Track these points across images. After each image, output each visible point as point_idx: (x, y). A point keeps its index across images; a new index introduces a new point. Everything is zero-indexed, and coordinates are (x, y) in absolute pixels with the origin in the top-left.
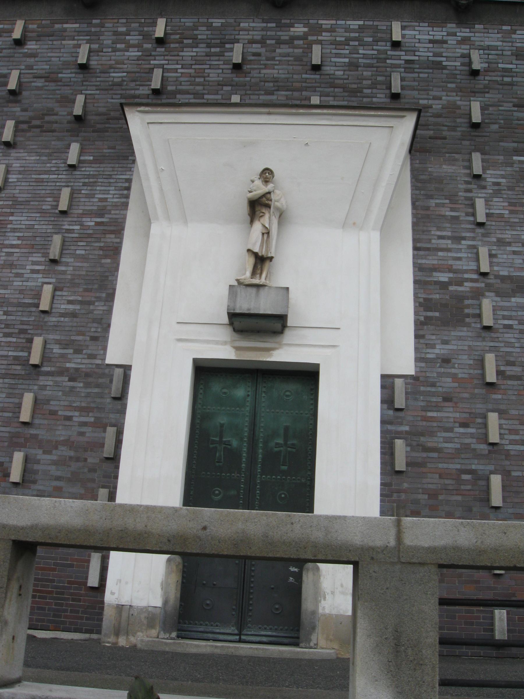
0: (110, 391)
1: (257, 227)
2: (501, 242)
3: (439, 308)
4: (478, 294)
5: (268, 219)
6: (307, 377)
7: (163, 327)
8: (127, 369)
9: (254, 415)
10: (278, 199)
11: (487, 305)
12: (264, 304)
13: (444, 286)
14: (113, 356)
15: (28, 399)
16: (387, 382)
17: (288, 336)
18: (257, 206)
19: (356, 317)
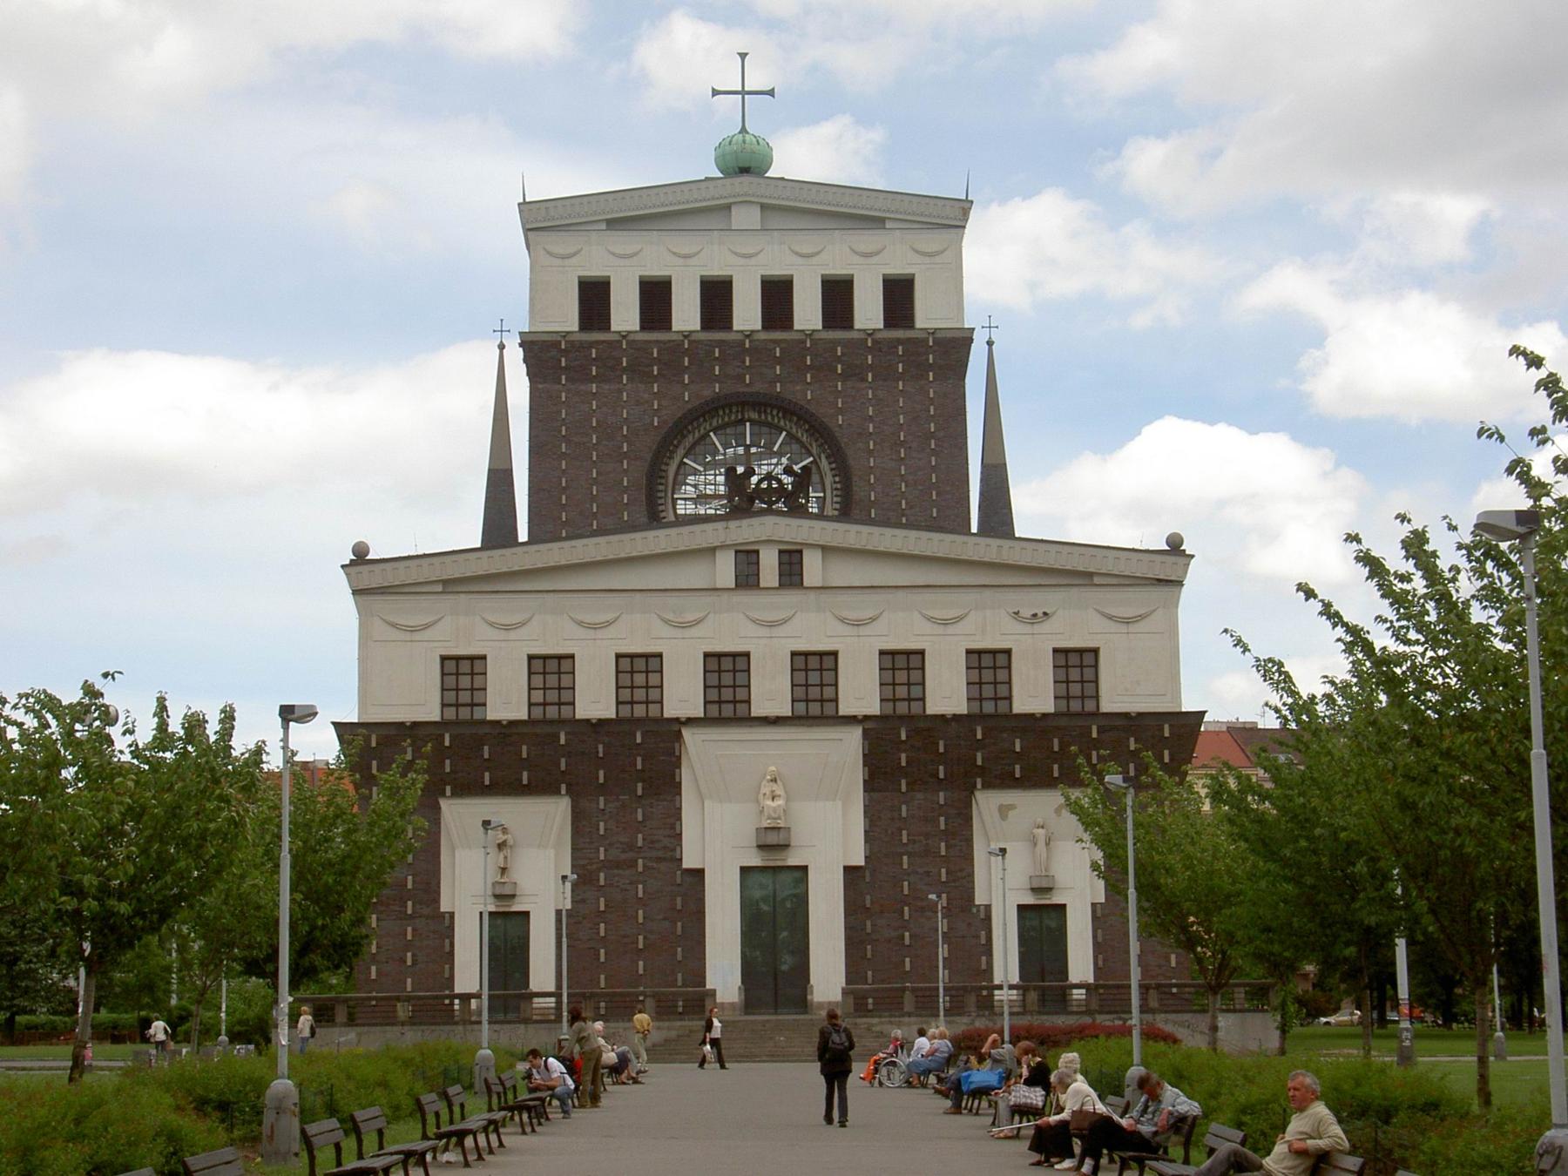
0: (445, 926)
1: (502, 856)
2: (611, 845)
3: (584, 877)
4: (599, 870)
5: (507, 851)
6: (526, 914)
7: (465, 892)
8: (452, 915)
9: (507, 935)
10: (510, 842)
11: (602, 875)
12: (507, 891)
13: (584, 866)
14: (445, 907)
15: (409, 929)
16: (559, 913)
17: (517, 899)
18: (501, 846)
19: (544, 886)
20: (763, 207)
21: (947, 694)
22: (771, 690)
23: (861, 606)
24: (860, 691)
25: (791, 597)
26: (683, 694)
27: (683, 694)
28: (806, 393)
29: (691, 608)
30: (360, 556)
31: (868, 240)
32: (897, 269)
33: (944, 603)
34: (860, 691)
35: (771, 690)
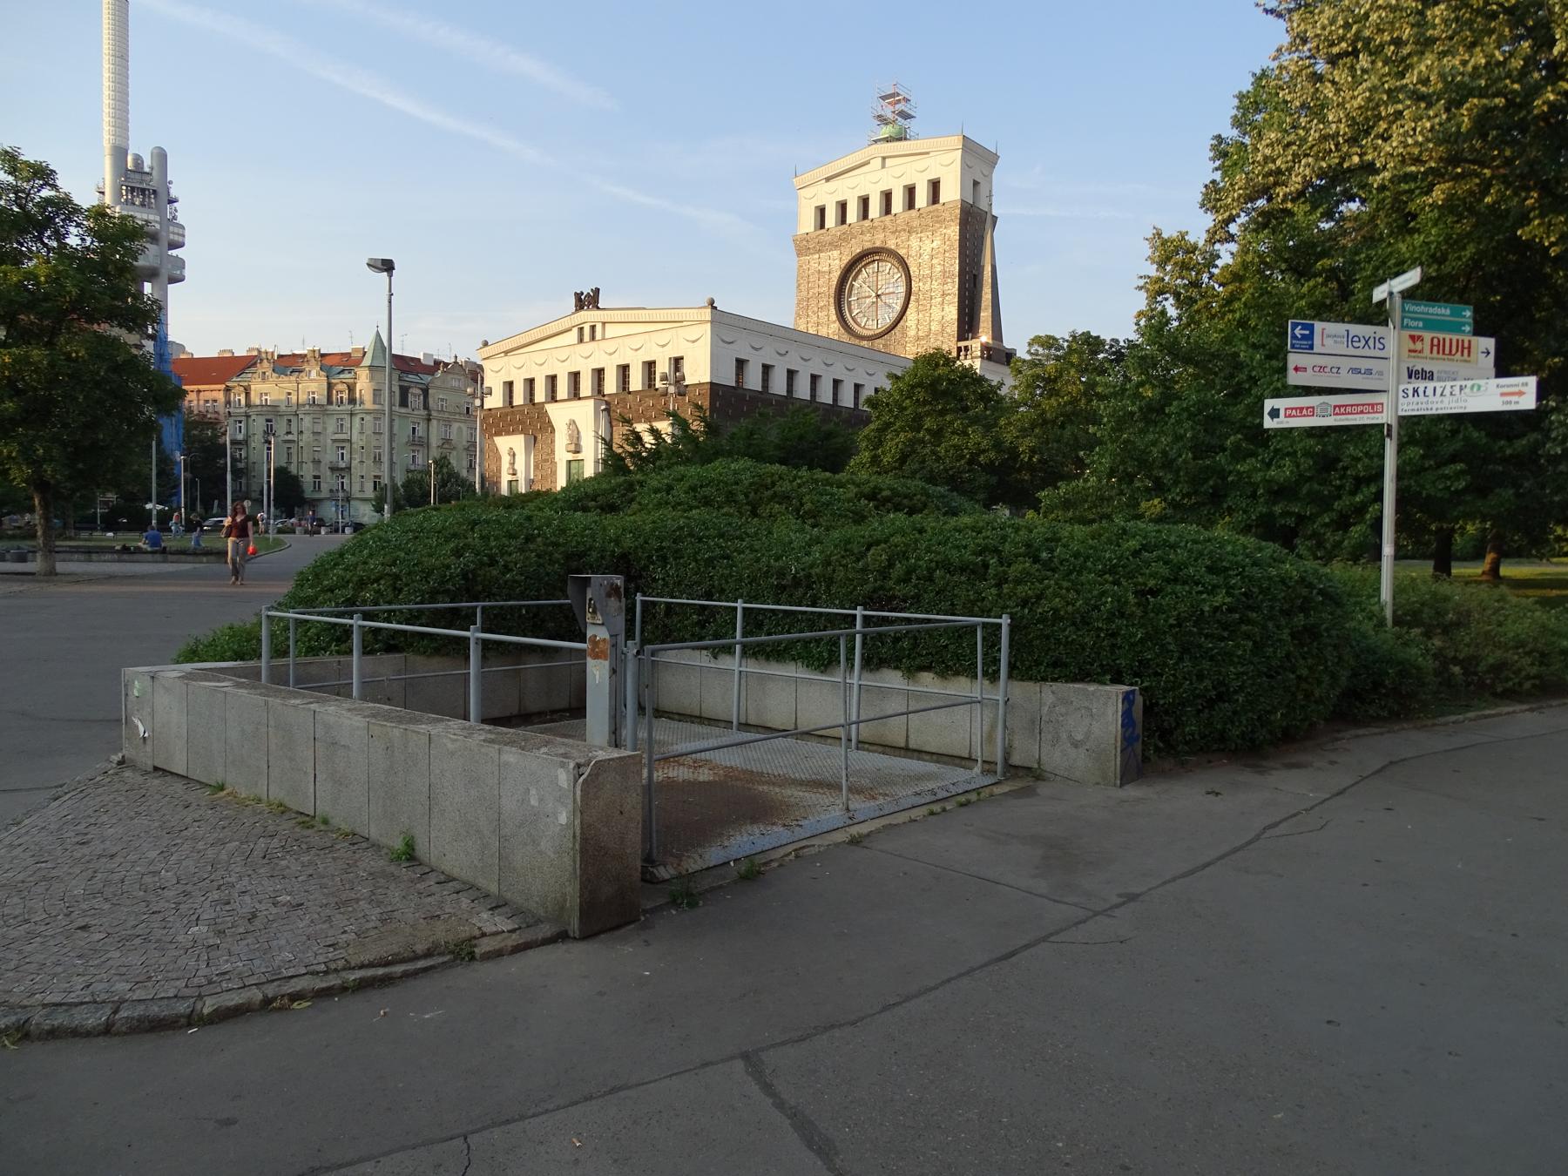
20: (884, 158)
21: (636, 382)
22: (586, 387)
23: (609, 346)
24: (611, 386)
25: (593, 344)
26: (563, 390)
27: (563, 390)
28: (891, 244)
29: (563, 354)
30: (486, 344)
31: (922, 163)
32: (933, 177)
33: (636, 342)
34: (611, 386)
35: (586, 387)
